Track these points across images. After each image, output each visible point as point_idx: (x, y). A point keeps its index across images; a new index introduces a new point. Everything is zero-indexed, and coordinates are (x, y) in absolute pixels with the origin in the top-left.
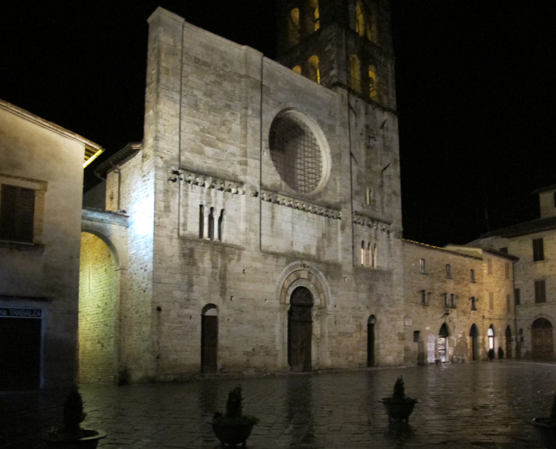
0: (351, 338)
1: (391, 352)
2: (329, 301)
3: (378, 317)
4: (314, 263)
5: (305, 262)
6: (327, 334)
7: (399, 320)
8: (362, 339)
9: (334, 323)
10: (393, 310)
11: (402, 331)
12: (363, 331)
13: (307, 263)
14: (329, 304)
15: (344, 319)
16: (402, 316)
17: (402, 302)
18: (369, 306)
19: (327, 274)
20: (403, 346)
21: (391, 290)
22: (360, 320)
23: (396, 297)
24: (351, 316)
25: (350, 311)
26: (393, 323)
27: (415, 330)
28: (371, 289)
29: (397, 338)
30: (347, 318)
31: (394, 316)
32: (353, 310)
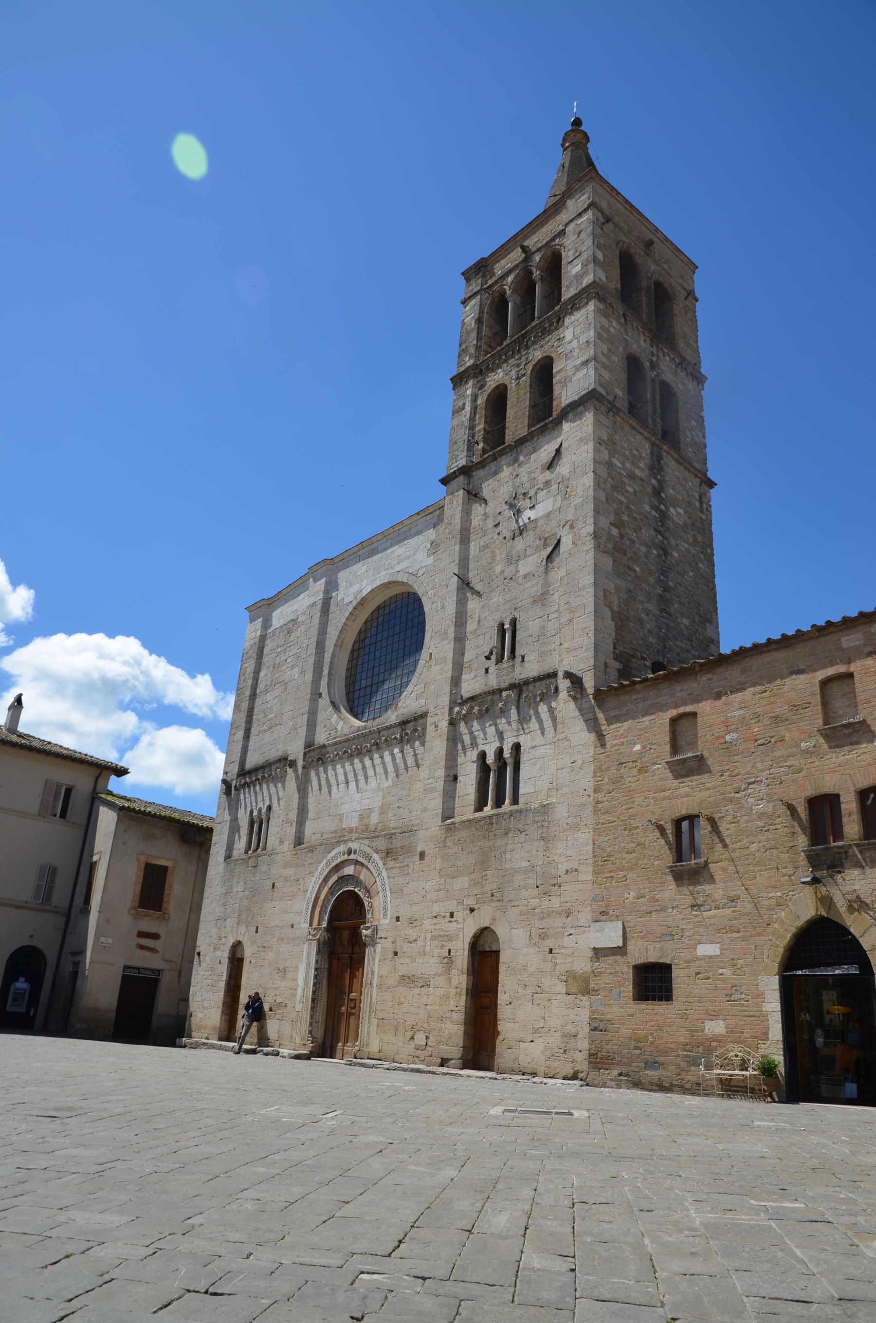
0: (424, 990)
1: (536, 1031)
2: (385, 909)
3: (501, 931)
4: (366, 842)
5: (350, 845)
6: (375, 984)
7: (572, 931)
8: (453, 992)
9: (391, 955)
10: (555, 902)
11: (582, 965)
12: (454, 971)
13: (354, 846)
14: (385, 915)
15: (414, 944)
16: (585, 917)
17: (586, 874)
18: (476, 907)
19: (388, 853)
20: (584, 1015)
21: (547, 849)
22: (449, 945)
23: (562, 868)
24: (429, 936)
25: (427, 924)
26: (549, 943)
27: (641, 961)
28: (484, 863)
29: (562, 988)
30: (420, 943)
31: (556, 923)
32: (435, 920)
